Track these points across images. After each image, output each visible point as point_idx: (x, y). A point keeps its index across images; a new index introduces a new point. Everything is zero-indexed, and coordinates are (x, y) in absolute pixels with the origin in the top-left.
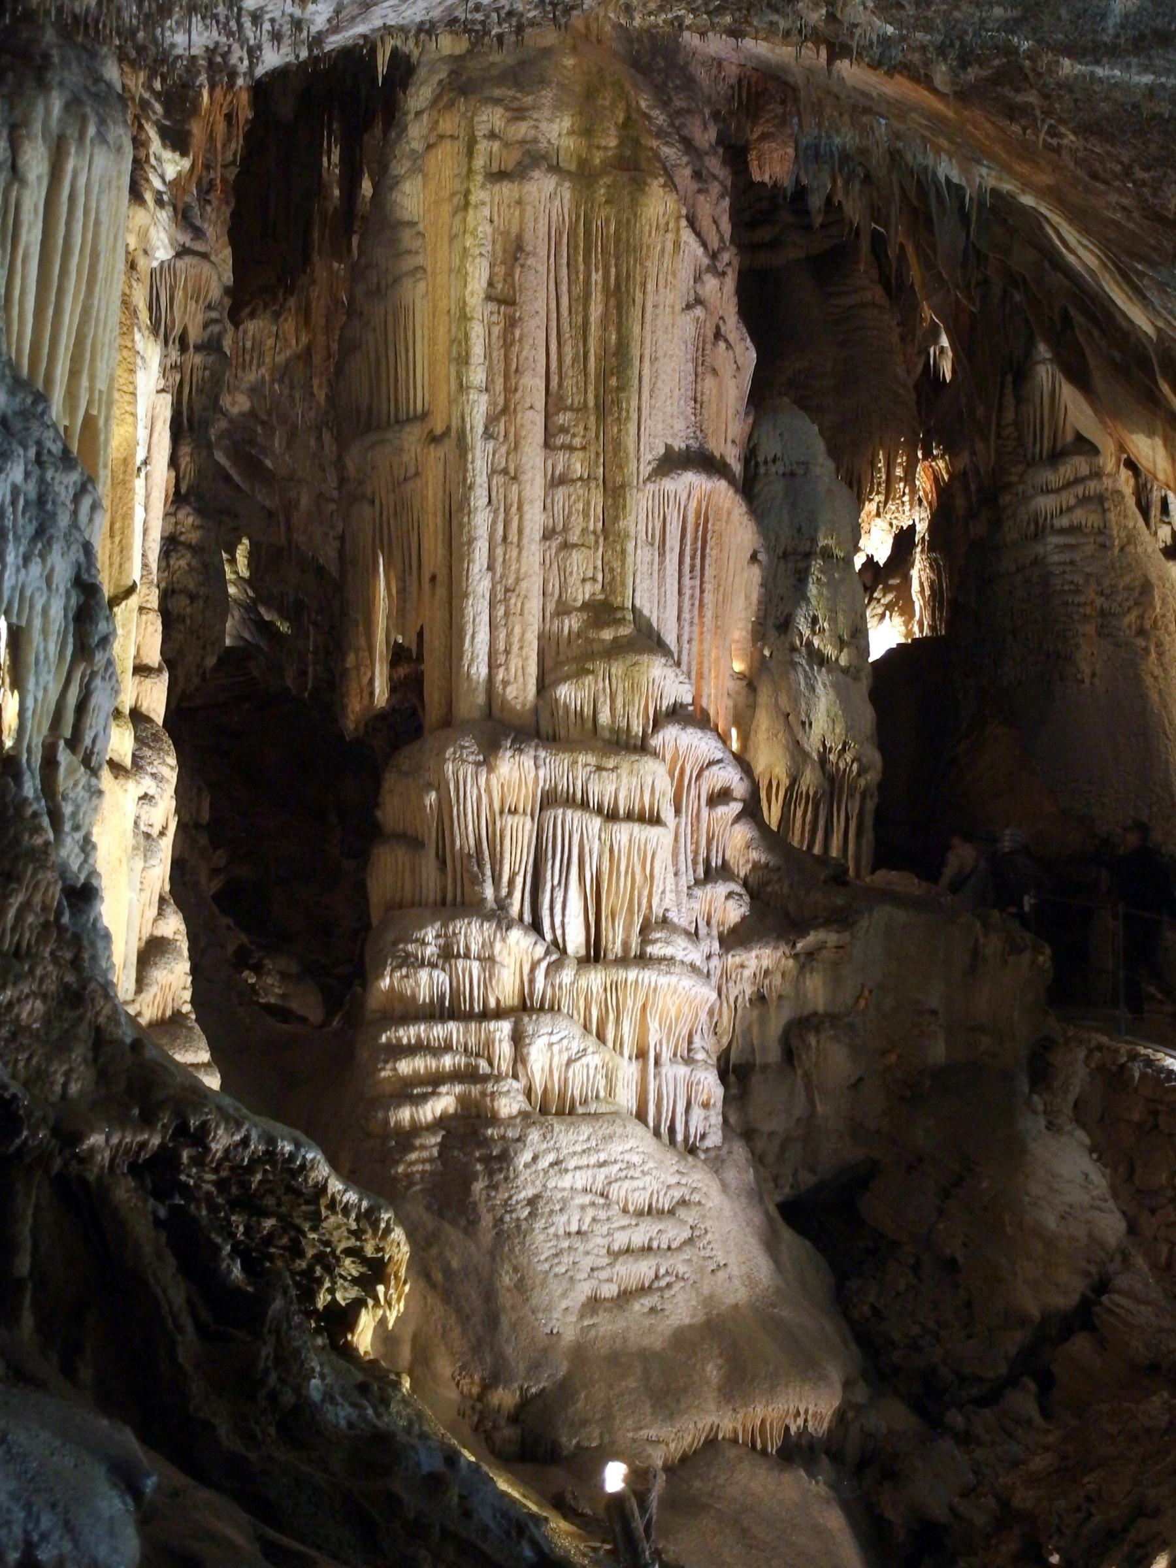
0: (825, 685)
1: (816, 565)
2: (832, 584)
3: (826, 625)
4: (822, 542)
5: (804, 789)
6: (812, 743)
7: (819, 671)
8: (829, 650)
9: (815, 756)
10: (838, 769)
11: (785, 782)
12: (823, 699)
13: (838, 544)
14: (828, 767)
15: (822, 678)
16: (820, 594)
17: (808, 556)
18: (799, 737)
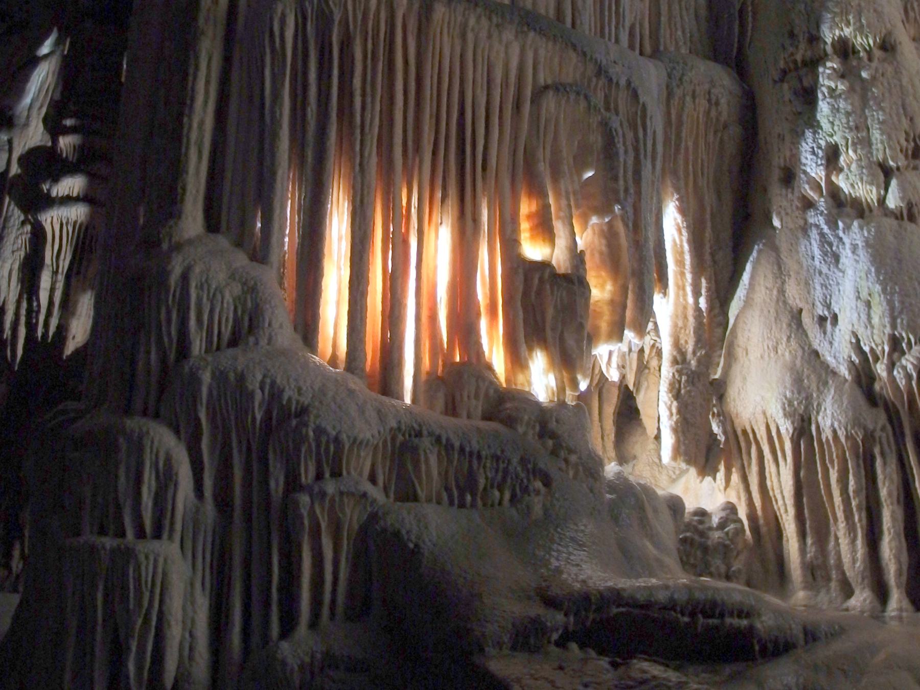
0: (854, 248)
1: (827, 78)
2: (861, 92)
3: (851, 152)
4: (829, 35)
5: (827, 434)
6: (838, 352)
7: (848, 228)
8: (867, 192)
9: (844, 371)
10: (896, 387)
11: (786, 427)
12: (850, 272)
13: (860, 29)
14: (877, 387)
15: (853, 237)
16: (835, 110)
17: (813, 63)
18: (816, 346)
